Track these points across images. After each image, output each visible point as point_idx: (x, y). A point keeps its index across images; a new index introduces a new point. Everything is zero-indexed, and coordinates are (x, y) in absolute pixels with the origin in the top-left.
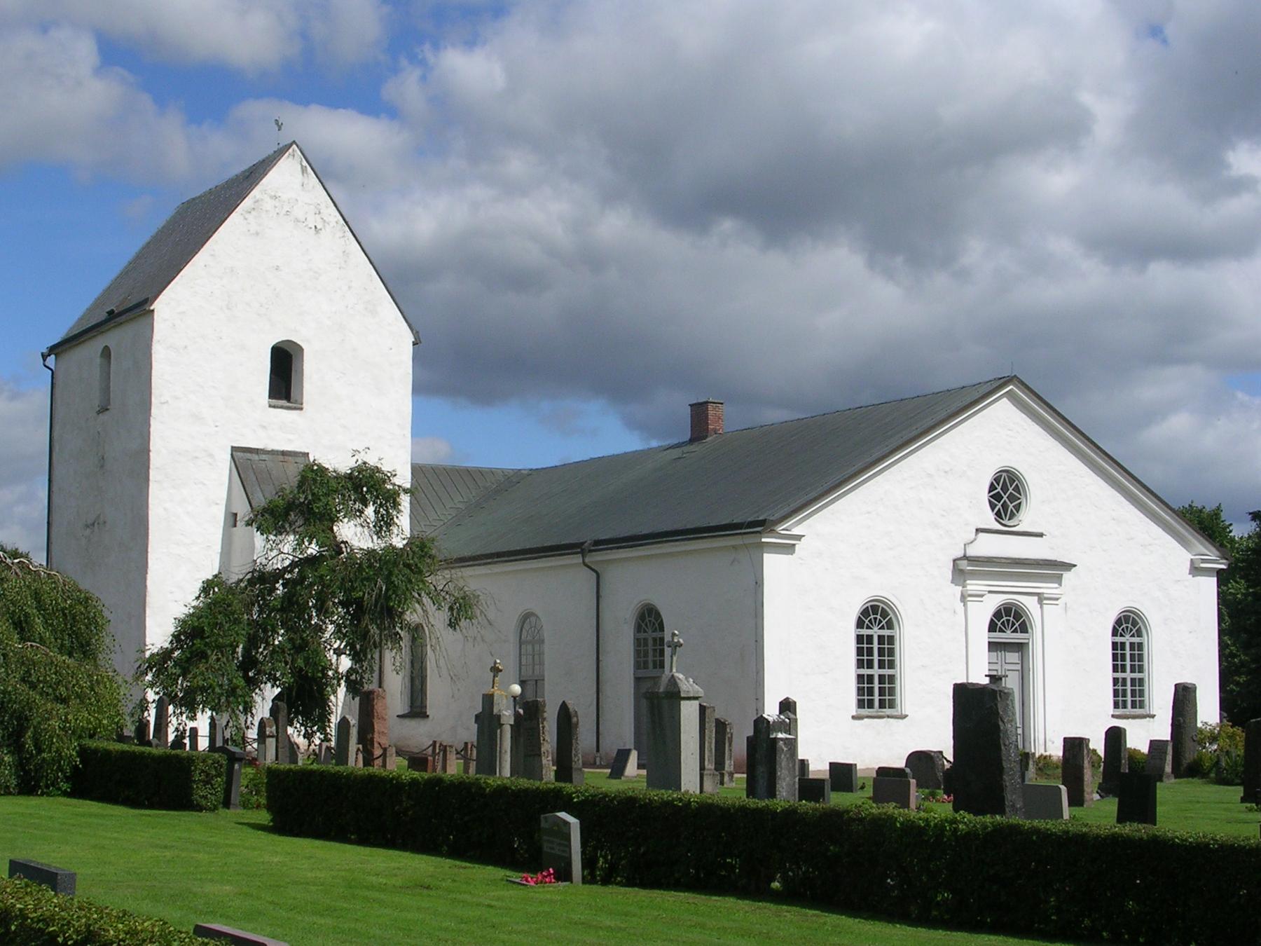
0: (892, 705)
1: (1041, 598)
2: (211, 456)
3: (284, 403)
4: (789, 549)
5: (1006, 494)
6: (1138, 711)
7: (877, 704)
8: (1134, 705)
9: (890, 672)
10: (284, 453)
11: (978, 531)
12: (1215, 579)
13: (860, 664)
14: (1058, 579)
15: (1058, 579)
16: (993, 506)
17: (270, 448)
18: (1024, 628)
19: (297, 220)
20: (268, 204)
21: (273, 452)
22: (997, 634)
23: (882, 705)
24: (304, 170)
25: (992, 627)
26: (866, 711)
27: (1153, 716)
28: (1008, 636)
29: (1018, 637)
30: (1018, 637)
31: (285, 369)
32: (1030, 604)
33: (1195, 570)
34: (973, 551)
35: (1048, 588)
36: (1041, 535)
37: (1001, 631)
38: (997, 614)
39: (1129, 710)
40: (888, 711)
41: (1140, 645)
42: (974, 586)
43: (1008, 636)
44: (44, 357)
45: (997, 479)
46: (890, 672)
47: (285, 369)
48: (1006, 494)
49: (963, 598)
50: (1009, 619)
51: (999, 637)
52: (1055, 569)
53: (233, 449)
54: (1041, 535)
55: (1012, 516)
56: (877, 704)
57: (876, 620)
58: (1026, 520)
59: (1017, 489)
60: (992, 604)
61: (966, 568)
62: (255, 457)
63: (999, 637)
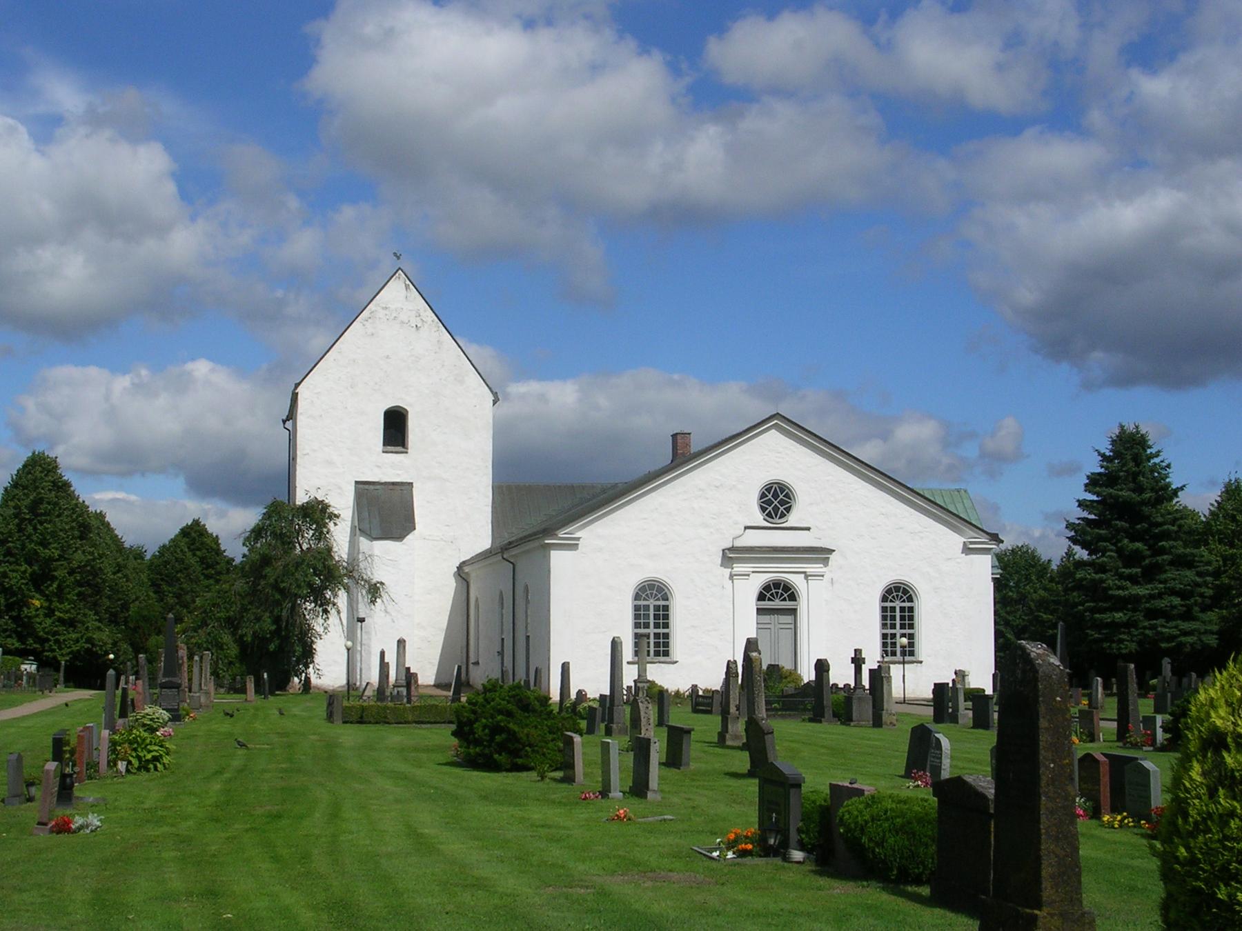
0: (666, 654)
1: (807, 576)
2: (340, 488)
3: (400, 449)
4: (574, 547)
5: (776, 500)
9: (665, 631)
10: (393, 484)
11: (746, 528)
13: (884, 626)
14: (825, 562)
15: (825, 562)
16: (763, 509)
17: (383, 480)
18: (793, 597)
19: (402, 322)
20: (381, 313)
21: (385, 483)
22: (767, 602)
23: (657, 654)
24: (407, 287)
25: (761, 597)
28: (777, 604)
29: (788, 604)
30: (788, 604)
31: (395, 427)
32: (797, 581)
33: (967, 550)
34: (738, 543)
35: (812, 568)
36: (808, 529)
37: (770, 600)
38: (767, 588)
40: (662, 659)
41: (911, 609)
42: (739, 568)
43: (777, 604)
44: (284, 422)
45: (769, 490)
46: (665, 631)
47: (395, 427)
48: (776, 500)
49: (731, 577)
51: (766, 604)
52: (821, 554)
53: (357, 482)
54: (808, 529)
55: (783, 516)
58: (793, 519)
59: (787, 496)
60: (757, 582)
61: (732, 555)
62: (372, 487)
63: (766, 604)
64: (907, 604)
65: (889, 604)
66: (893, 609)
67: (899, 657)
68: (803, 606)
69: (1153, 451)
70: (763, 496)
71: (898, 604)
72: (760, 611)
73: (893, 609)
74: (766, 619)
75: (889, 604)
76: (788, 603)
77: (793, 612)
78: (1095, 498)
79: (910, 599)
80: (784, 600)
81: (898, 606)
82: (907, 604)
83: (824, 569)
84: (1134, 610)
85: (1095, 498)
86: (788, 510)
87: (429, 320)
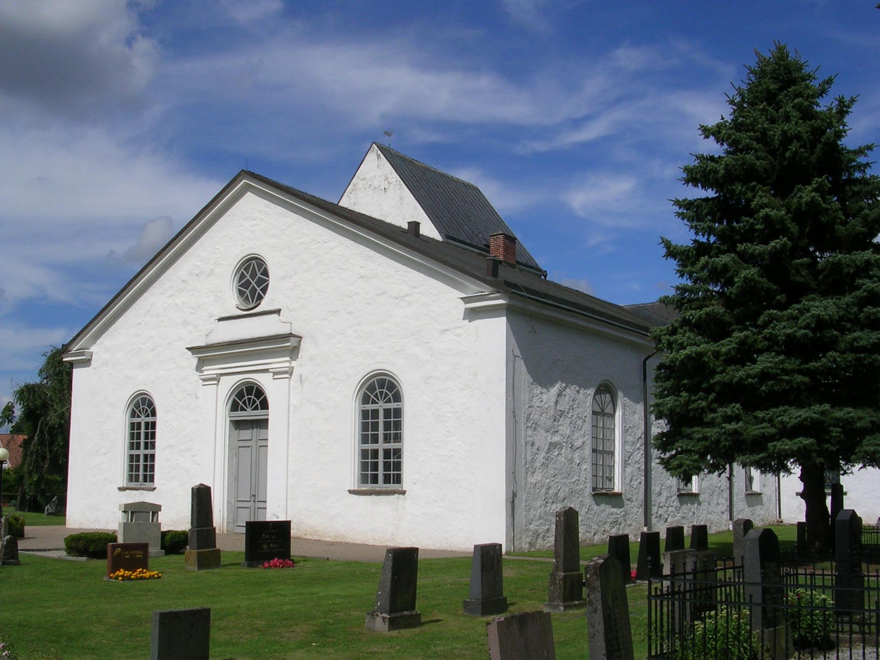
4: (87, 363)
5: (253, 279)
6: (392, 486)
7: (141, 478)
8: (387, 480)
11: (220, 320)
12: (504, 319)
14: (294, 352)
16: (241, 293)
18: (265, 405)
24: (378, 156)
25: (235, 407)
26: (133, 485)
27: (404, 493)
28: (250, 414)
29: (258, 414)
30: (258, 414)
32: (265, 381)
33: (472, 314)
35: (280, 363)
36: (278, 312)
37: (243, 409)
39: (381, 485)
42: (211, 370)
43: (250, 414)
48: (253, 279)
50: (249, 401)
51: (241, 415)
52: (286, 344)
55: (260, 298)
56: (141, 478)
57: (143, 408)
60: (228, 384)
61: (206, 354)
63: (241, 415)
64: (392, 405)
65: (370, 407)
66: (375, 413)
68: (274, 414)
69: (815, 84)
70: (242, 276)
71: (381, 406)
72: (238, 425)
73: (375, 413)
74: (246, 434)
75: (370, 407)
76: (260, 412)
77: (263, 424)
78: (711, 193)
79: (397, 397)
80: (256, 408)
81: (381, 407)
82: (392, 405)
83: (294, 363)
84: (693, 390)
85: (711, 193)
86: (265, 290)
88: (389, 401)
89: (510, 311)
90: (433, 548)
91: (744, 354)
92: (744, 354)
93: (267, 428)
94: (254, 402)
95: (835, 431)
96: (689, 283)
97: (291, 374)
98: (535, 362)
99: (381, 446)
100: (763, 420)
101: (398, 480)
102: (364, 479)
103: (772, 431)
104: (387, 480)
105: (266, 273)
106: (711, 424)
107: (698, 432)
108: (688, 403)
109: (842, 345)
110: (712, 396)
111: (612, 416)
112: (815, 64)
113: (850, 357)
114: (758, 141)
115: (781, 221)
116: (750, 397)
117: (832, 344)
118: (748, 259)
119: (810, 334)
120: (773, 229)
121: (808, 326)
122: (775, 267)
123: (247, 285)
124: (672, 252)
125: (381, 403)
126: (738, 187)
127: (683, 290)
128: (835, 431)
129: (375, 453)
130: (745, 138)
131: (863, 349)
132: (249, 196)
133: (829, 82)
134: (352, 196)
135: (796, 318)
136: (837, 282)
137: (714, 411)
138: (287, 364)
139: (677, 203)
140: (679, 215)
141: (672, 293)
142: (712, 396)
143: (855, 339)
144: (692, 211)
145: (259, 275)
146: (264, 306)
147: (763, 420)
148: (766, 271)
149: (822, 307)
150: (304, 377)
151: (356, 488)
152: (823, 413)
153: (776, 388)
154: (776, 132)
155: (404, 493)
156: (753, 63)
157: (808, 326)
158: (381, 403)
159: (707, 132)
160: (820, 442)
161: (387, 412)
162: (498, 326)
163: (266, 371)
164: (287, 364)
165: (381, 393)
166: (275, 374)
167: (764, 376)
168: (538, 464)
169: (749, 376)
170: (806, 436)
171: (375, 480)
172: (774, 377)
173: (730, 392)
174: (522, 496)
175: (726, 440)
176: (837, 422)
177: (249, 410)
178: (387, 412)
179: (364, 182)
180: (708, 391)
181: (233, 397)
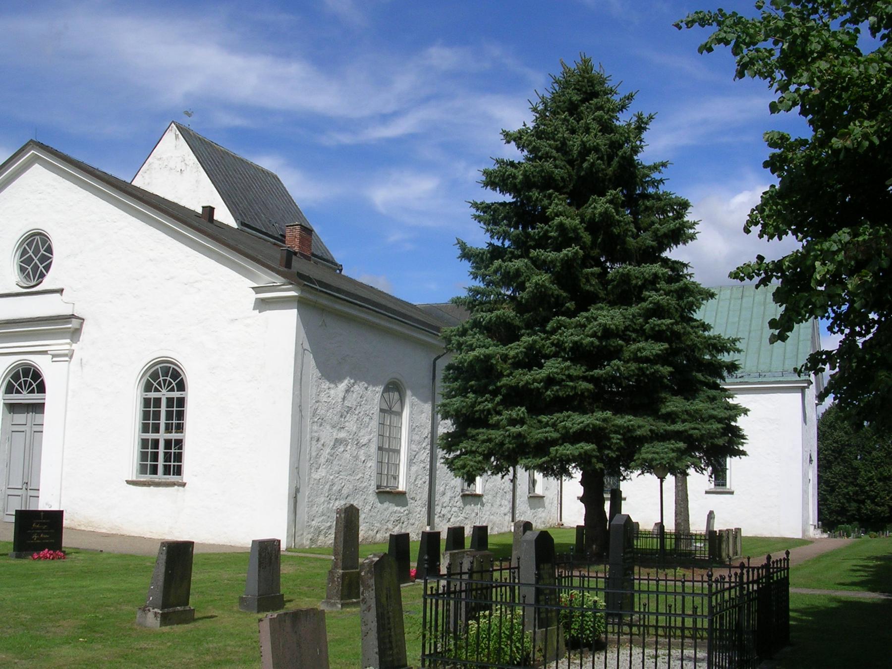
5: (36, 255)
6: (172, 478)
8: (167, 471)
12: (294, 312)
14: (75, 334)
16: (22, 270)
18: (41, 388)
22: (14, 396)
24: (177, 136)
25: (10, 389)
27: (184, 485)
28: (25, 397)
29: (34, 398)
30: (34, 398)
32: (42, 363)
33: (263, 305)
35: (60, 345)
36: (60, 291)
37: (18, 392)
43: (25, 397)
48: (36, 255)
51: (15, 398)
52: (67, 326)
55: (42, 276)
63: (15, 398)
64: (176, 394)
65: (153, 395)
66: (158, 401)
67: (160, 476)
68: (50, 398)
69: (616, 99)
70: (24, 252)
71: (164, 394)
72: (12, 408)
73: (158, 401)
74: (20, 418)
75: (153, 395)
76: (36, 395)
77: (39, 408)
78: (508, 198)
79: (181, 386)
80: (32, 392)
81: (164, 395)
83: (74, 346)
84: (480, 391)
85: (508, 198)
86: (47, 268)
87: (191, 163)
88: (172, 390)
89: (302, 304)
90: (212, 542)
91: (532, 359)
92: (532, 359)
93: (43, 413)
94: (31, 384)
95: (616, 438)
96: (482, 285)
97: (71, 357)
98: (325, 356)
99: (162, 436)
100: (547, 425)
101: (178, 471)
102: (143, 470)
103: (555, 435)
104: (167, 471)
105: (49, 250)
106: (496, 426)
107: (483, 433)
108: (473, 405)
109: (626, 355)
110: (498, 398)
111: (400, 414)
112: (617, 79)
113: (633, 366)
114: (558, 150)
115: (575, 230)
116: (534, 401)
117: (616, 353)
118: (540, 265)
119: (597, 342)
120: (566, 238)
121: (594, 335)
122: (566, 275)
123: (29, 261)
124: (467, 254)
125: (164, 391)
126: (535, 194)
127: (476, 292)
128: (616, 438)
129: (156, 443)
130: (545, 146)
131: (646, 360)
132: (37, 168)
133: (630, 98)
134: (146, 175)
135: (584, 326)
136: (625, 293)
137: (499, 413)
138: (67, 347)
139: (475, 205)
140: (476, 217)
141: (464, 294)
142: (498, 398)
143: (639, 350)
144: (489, 215)
145: (42, 251)
146: (46, 284)
147: (547, 425)
148: (558, 279)
149: (608, 316)
150: (84, 361)
151: (134, 479)
152: (605, 420)
153: (561, 394)
154: (575, 143)
155: (184, 485)
156: (558, 73)
157: (594, 335)
158: (164, 391)
159: (508, 137)
160: (601, 448)
161: (170, 401)
162: (289, 318)
163: (45, 353)
164: (67, 347)
165: (165, 381)
166: (54, 356)
167: (550, 381)
168: (322, 460)
169: (535, 380)
170: (588, 441)
171: (154, 470)
172: (559, 383)
173: (517, 396)
174: (305, 492)
175: (510, 443)
176: (618, 430)
177: (25, 392)
178: (170, 401)
179: (160, 162)
180: (495, 393)
181: (9, 378)
